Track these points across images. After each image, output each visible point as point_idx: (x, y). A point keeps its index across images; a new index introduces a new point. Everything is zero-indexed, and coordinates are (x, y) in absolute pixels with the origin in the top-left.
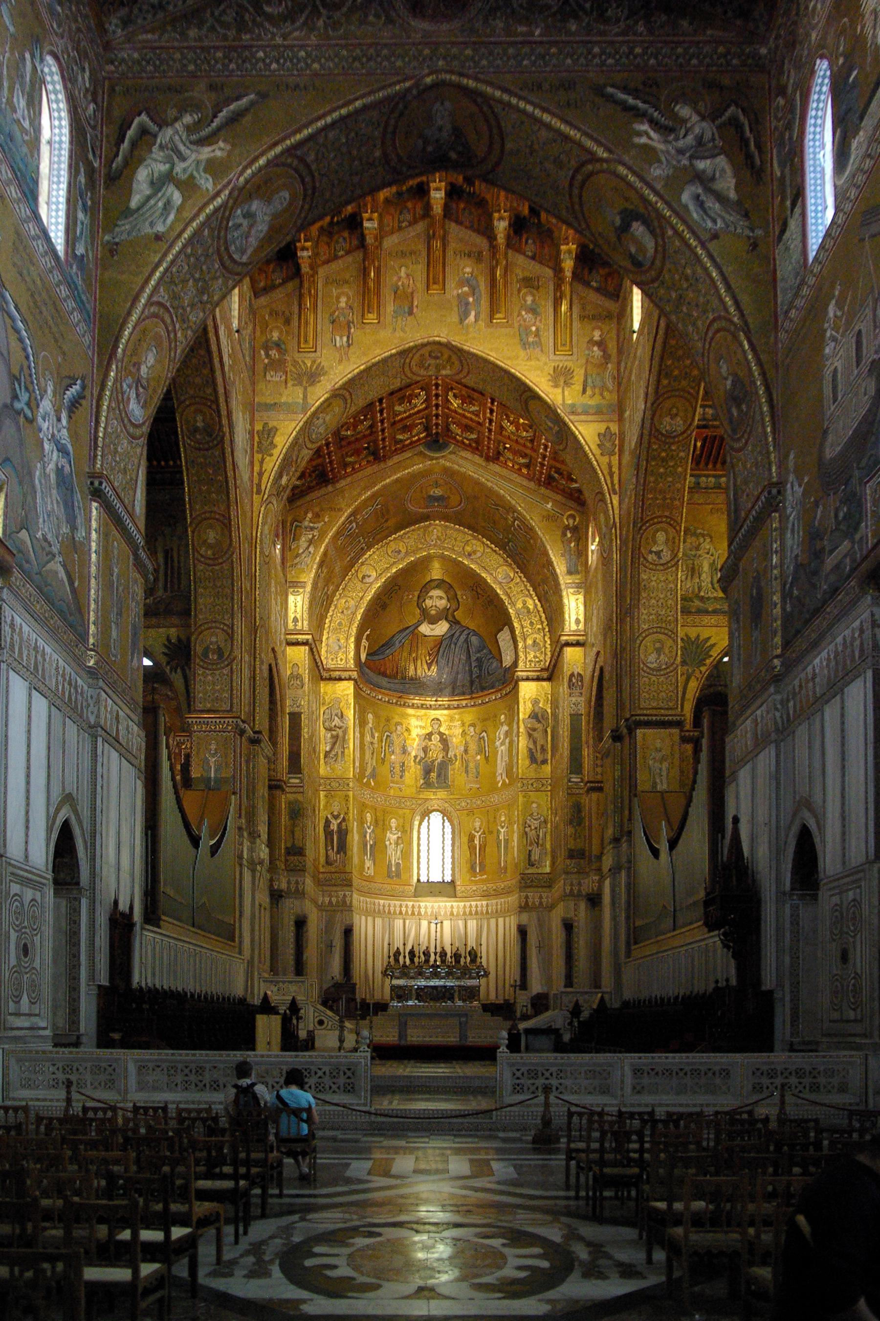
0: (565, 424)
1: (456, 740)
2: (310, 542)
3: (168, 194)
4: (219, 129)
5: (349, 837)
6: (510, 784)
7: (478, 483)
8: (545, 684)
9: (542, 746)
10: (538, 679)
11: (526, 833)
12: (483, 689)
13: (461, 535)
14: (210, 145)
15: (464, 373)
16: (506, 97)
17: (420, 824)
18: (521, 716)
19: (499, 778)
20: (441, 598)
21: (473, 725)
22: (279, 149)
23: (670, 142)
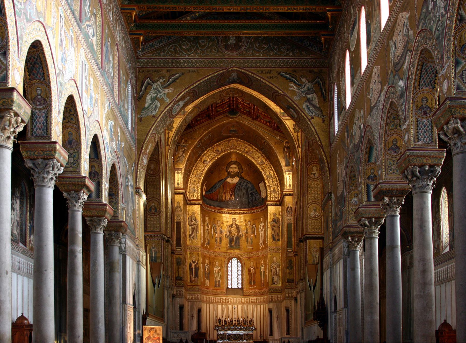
0: (281, 120)
1: (243, 228)
2: (184, 152)
3: (156, 103)
4: (170, 84)
5: (199, 271)
6: (265, 248)
7: (249, 127)
8: (278, 207)
9: (278, 233)
10: (275, 205)
11: (271, 270)
12: (253, 206)
13: (243, 144)
14: (168, 89)
15: (244, 96)
16: (253, 75)
17: (228, 264)
18: (269, 221)
19: (260, 245)
20: (236, 168)
21: (249, 221)
22: (187, 90)
23: (299, 89)
